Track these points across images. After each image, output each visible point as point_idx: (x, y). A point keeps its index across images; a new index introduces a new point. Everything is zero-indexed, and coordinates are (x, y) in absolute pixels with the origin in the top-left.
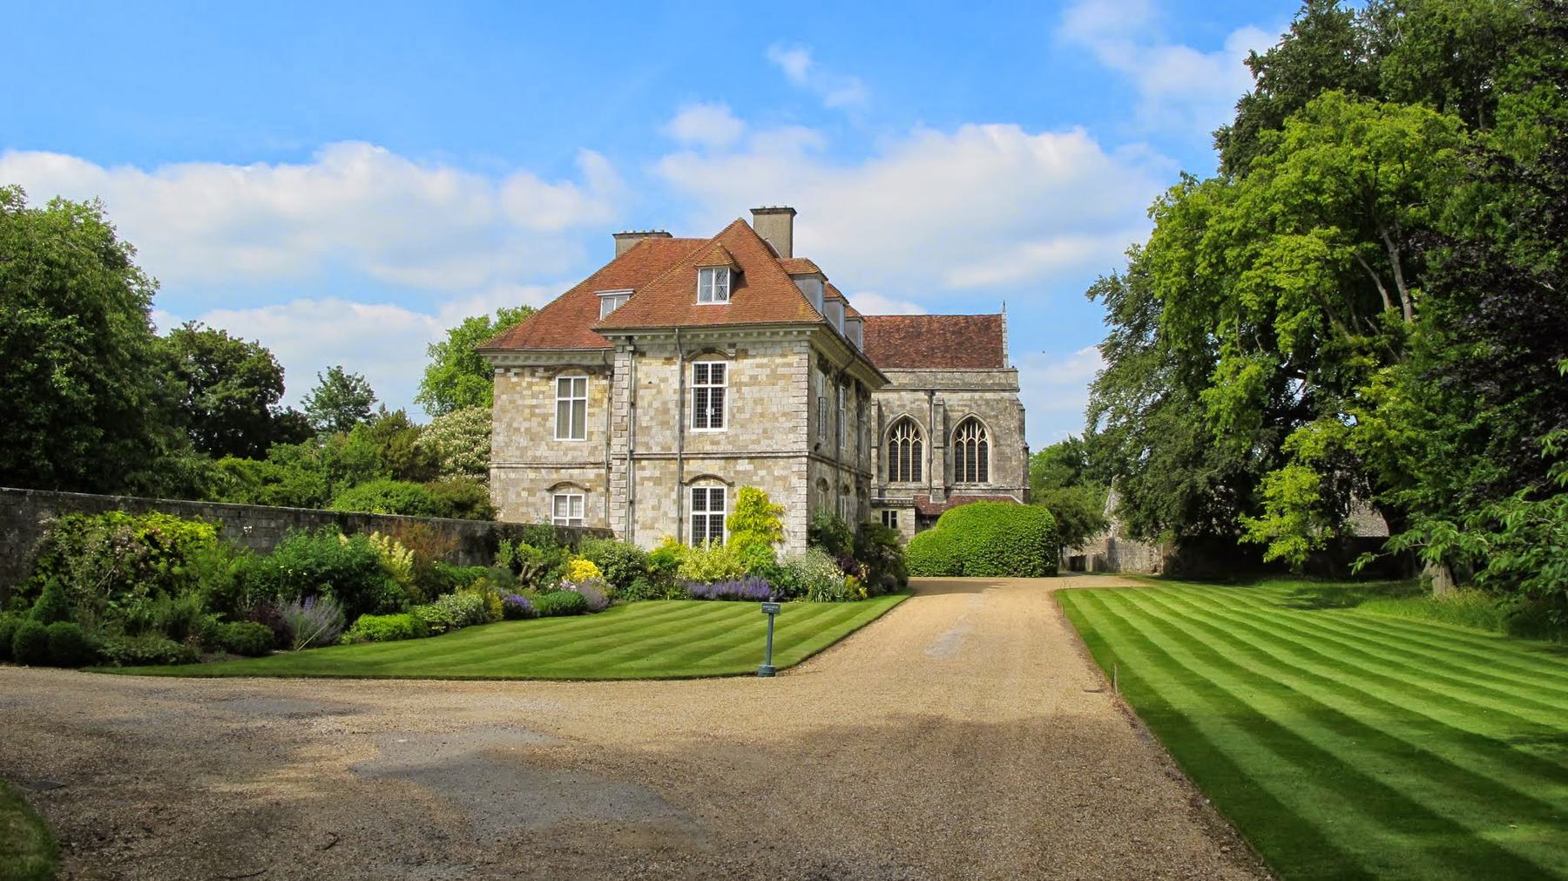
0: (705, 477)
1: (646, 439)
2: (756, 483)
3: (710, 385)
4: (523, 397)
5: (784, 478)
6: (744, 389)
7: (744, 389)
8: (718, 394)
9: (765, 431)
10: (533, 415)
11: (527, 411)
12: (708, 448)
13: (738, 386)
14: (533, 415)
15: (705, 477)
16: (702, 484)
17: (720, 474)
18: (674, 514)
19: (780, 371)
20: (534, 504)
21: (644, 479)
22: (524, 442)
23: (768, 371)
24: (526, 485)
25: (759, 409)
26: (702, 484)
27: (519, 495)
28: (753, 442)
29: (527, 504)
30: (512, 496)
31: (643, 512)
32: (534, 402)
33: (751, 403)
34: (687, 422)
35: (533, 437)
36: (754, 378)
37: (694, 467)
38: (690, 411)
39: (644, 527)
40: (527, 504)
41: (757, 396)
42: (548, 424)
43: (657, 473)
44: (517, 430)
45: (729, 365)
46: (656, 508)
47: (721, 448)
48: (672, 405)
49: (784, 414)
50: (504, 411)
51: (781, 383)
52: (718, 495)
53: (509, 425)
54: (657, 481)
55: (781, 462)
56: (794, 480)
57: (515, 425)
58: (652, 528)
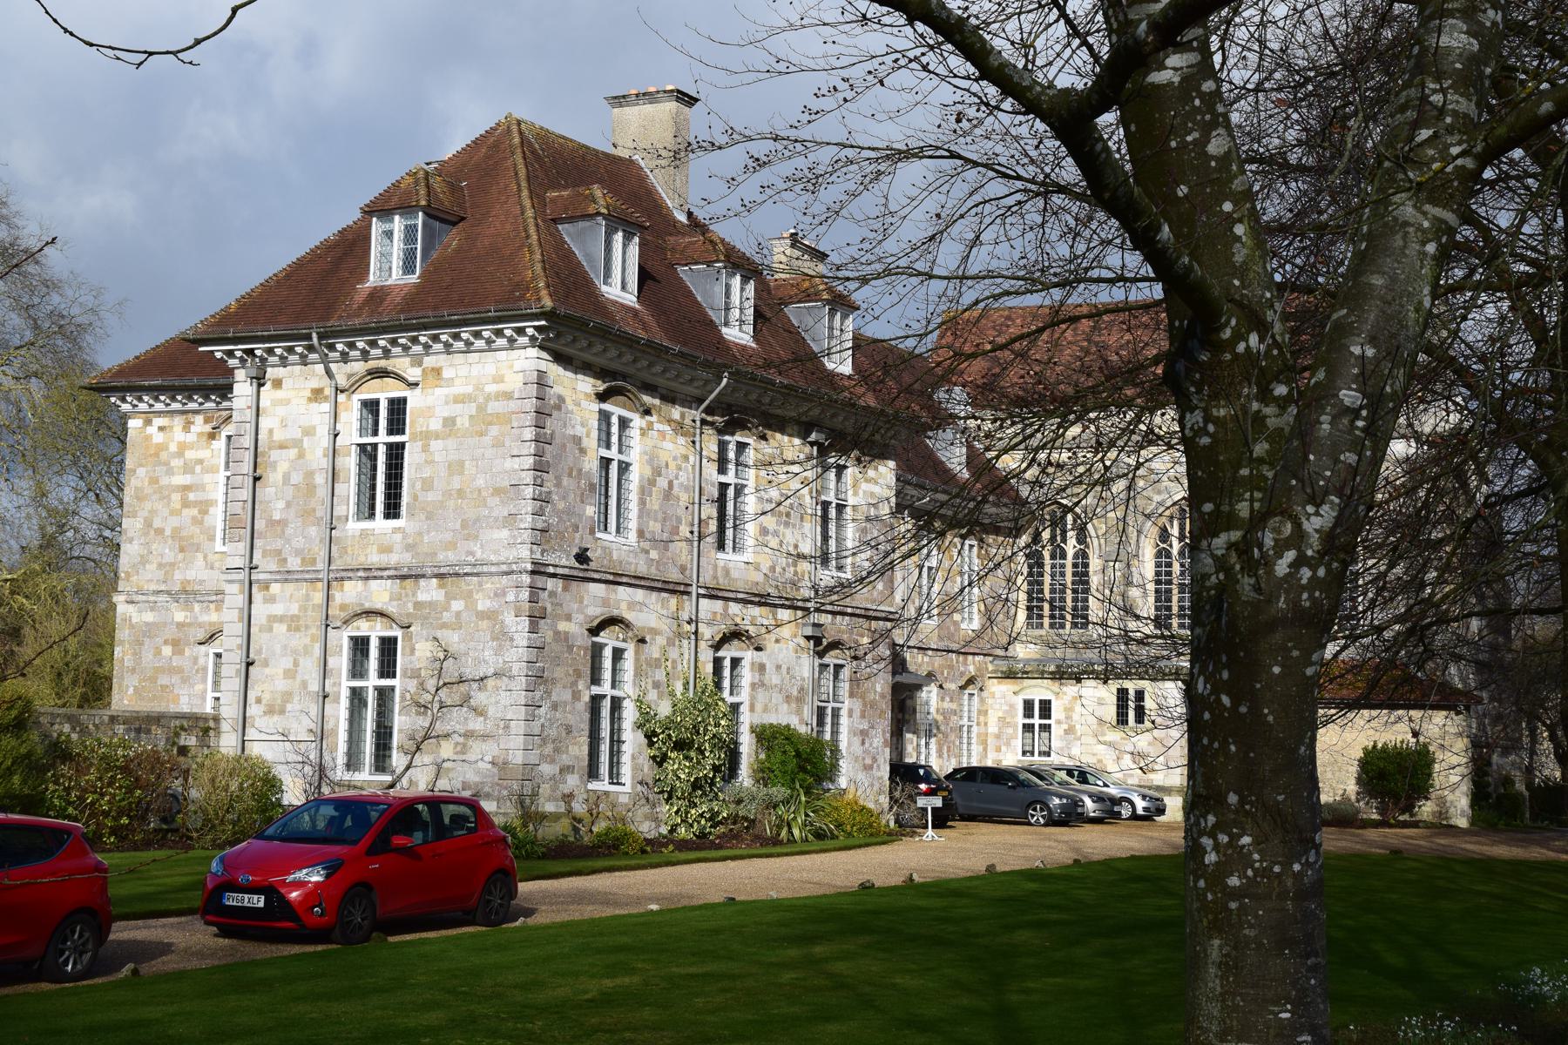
0: (369, 613)
1: (278, 544)
2: (444, 626)
3: (383, 438)
5: (490, 615)
6: (436, 445)
8: (396, 452)
9: (464, 525)
10: (186, 504)
11: (176, 497)
12: (375, 559)
13: (427, 436)
14: (186, 504)
15: (369, 613)
16: (363, 628)
17: (392, 609)
18: (314, 686)
19: (494, 407)
20: (179, 670)
21: (273, 619)
22: (169, 555)
23: (472, 408)
24: (171, 632)
25: (456, 483)
26: (363, 628)
27: (158, 652)
28: (451, 545)
29: (172, 670)
30: (147, 655)
31: (268, 682)
32: (186, 480)
34: (339, 510)
35: (186, 546)
36: (449, 422)
37: (351, 593)
38: (349, 488)
39: (270, 711)
40: (172, 670)
41: (453, 457)
42: (208, 520)
43: (294, 609)
44: (160, 531)
45: (414, 400)
46: (290, 674)
47: (393, 559)
48: (321, 479)
49: (498, 491)
51: (494, 431)
52: (388, 646)
53: (148, 524)
54: (294, 623)
55: (490, 585)
56: (509, 618)
57: (157, 523)
58: (282, 712)
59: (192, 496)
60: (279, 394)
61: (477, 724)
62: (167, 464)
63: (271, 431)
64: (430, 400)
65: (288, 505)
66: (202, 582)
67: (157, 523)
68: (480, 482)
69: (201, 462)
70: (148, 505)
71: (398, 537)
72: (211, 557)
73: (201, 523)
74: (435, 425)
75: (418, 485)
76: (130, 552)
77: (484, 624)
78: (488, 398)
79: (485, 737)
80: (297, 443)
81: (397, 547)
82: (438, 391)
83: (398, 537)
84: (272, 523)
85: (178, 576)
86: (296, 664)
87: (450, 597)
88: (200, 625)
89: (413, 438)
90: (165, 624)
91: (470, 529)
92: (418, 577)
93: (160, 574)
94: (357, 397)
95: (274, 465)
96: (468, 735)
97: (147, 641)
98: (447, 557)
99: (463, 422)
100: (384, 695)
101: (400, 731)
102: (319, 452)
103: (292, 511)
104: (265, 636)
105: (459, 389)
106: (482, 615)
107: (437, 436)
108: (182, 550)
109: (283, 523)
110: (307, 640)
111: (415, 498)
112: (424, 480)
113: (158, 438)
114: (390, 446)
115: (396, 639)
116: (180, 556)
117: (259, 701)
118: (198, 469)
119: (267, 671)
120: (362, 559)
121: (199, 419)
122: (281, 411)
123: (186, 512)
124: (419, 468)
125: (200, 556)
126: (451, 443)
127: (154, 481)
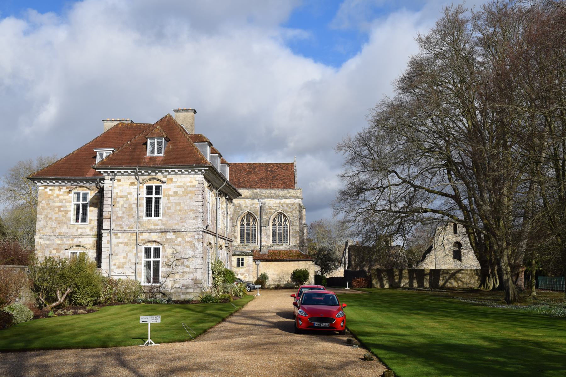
0: (151, 241)
1: (120, 223)
2: (176, 245)
4: (54, 202)
6: (171, 198)
7: (171, 198)
8: (157, 200)
9: (181, 219)
11: (56, 209)
12: (152, 227)
13: (168, 196)
14: (60, 211)
15: (151, 241)
16: (149, 245)
17: (159, 240)
19: (189, 189)
21: (119, 243)
22: (54, 225)
23: (183, 189)
24: (56, 246)
25: (178, 208)
31: (119, 259)
32: (60, 204)
33: (174, 205)
34: (140, 214)
35: (60, 222)
36: (176, 193)
37: (145, 236)
38: (144, 209)
39: (119, 267)
41: (177, 201)
43: (126, 240)
44: (51, 218)
45: (164, 186)
47: (159, 227)
48: (134, 206)
49: (191, 210)
50: (43, 209)
51: (190, 195)
52: (157, 251)
53: (46, 216)
54: (126, 244)
55: (189, 234)
56: (196, 243)
57: (50, 216)
58: (123, 267)
59: (62, 209)
60: (119, 183)
61: (187, 270)
62: (53, 200)
63: (117, 193)
64: (169, 187)
65: (123, 213)
66: (66, 233)
67: (50, 216)
68: (186, 208)
69: (65, 199)
70: (46, 211)
71: (160, 222)
72: (69, 226)
73: (65, 216)
74: (171, 193)
75: (166, 208)
76: (39, 225)
77: (188, 244)
78: (188, 187)
79: (189, 273)
80: (126, 196)
81: (160, 224)
82: (172, 184)
83: (160, 222)
84: (118, 217)
85: (57, 231)
86: (127, 255)
87: (177, 237)
88: (66, 245)
89: (164, 196)
90: (53, 244)
91: (182, 220)
92: (167, 232)
93: (51, 230)
94: (145, 185)
95: (118, 202)
96: (184, 273)
97: (47, 249)
98: (176, 227)
99: (180, 192)
100: (157, 264)
101: (162, 272)
102: (134, 199)
103: (125, 215)
104: (116, 247)
105: (178, 184)
106: (187, 242)
107: (172, 196)
108: (59, 224)
109: (122, 218)
110: (131, 249)
111: (165, 212)
112: (168, 207)
113: (50, 193)
114: (156, 198)
115: (159, 248)
116: (58, 225)
117: (115, 265)
118: (64, 201)
119: (117, 257)
120: (149, 227)
121: (64, 188)
122: (120, 188)
123: (60, 213)
124: (166, 204)
125: (65, 225)
126: (176, 198)
127: (48, 204)
